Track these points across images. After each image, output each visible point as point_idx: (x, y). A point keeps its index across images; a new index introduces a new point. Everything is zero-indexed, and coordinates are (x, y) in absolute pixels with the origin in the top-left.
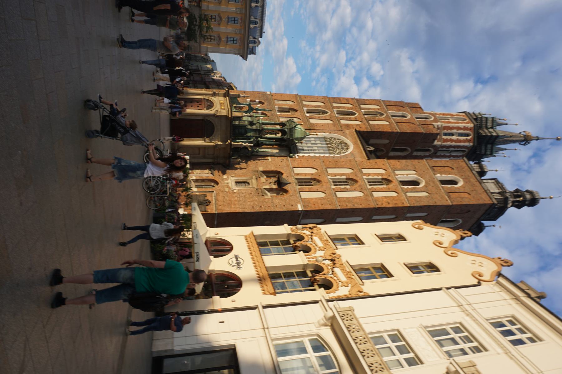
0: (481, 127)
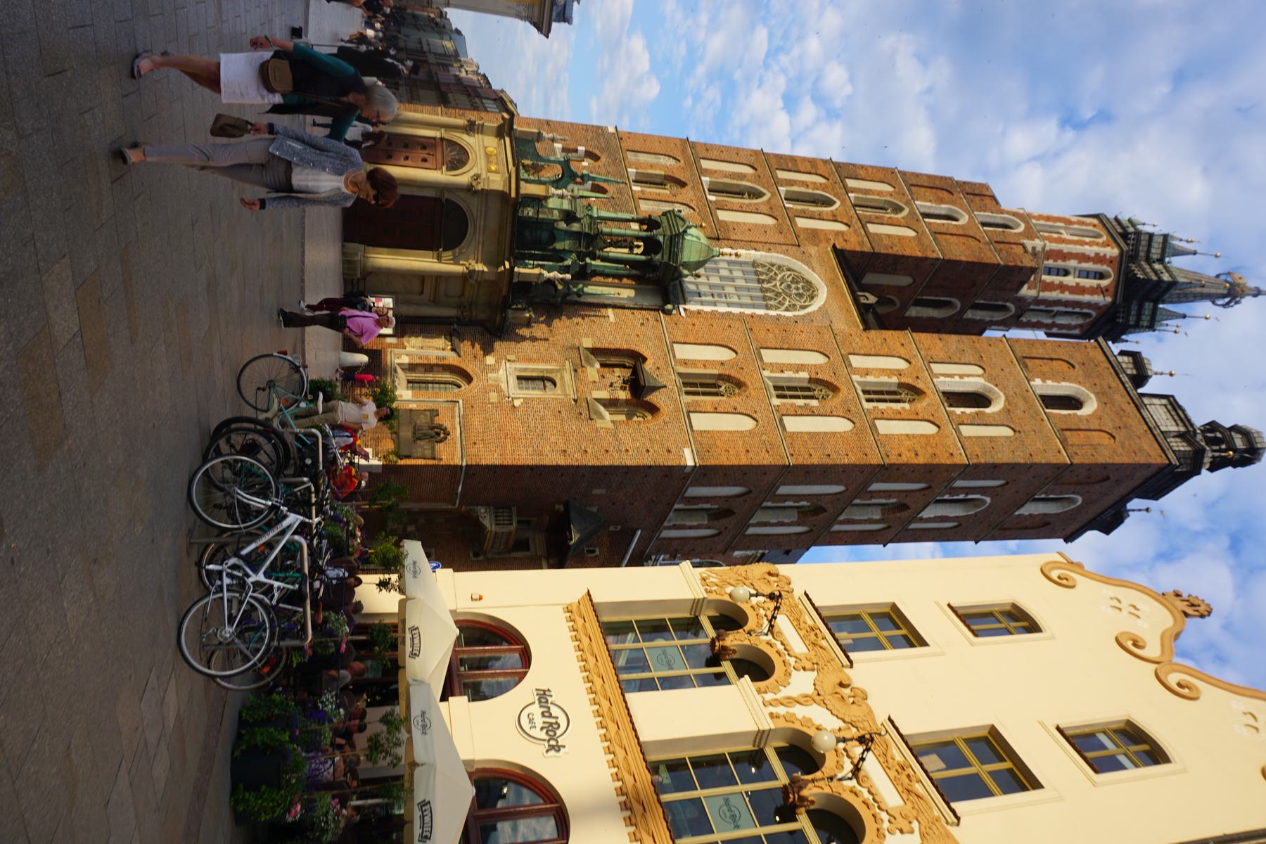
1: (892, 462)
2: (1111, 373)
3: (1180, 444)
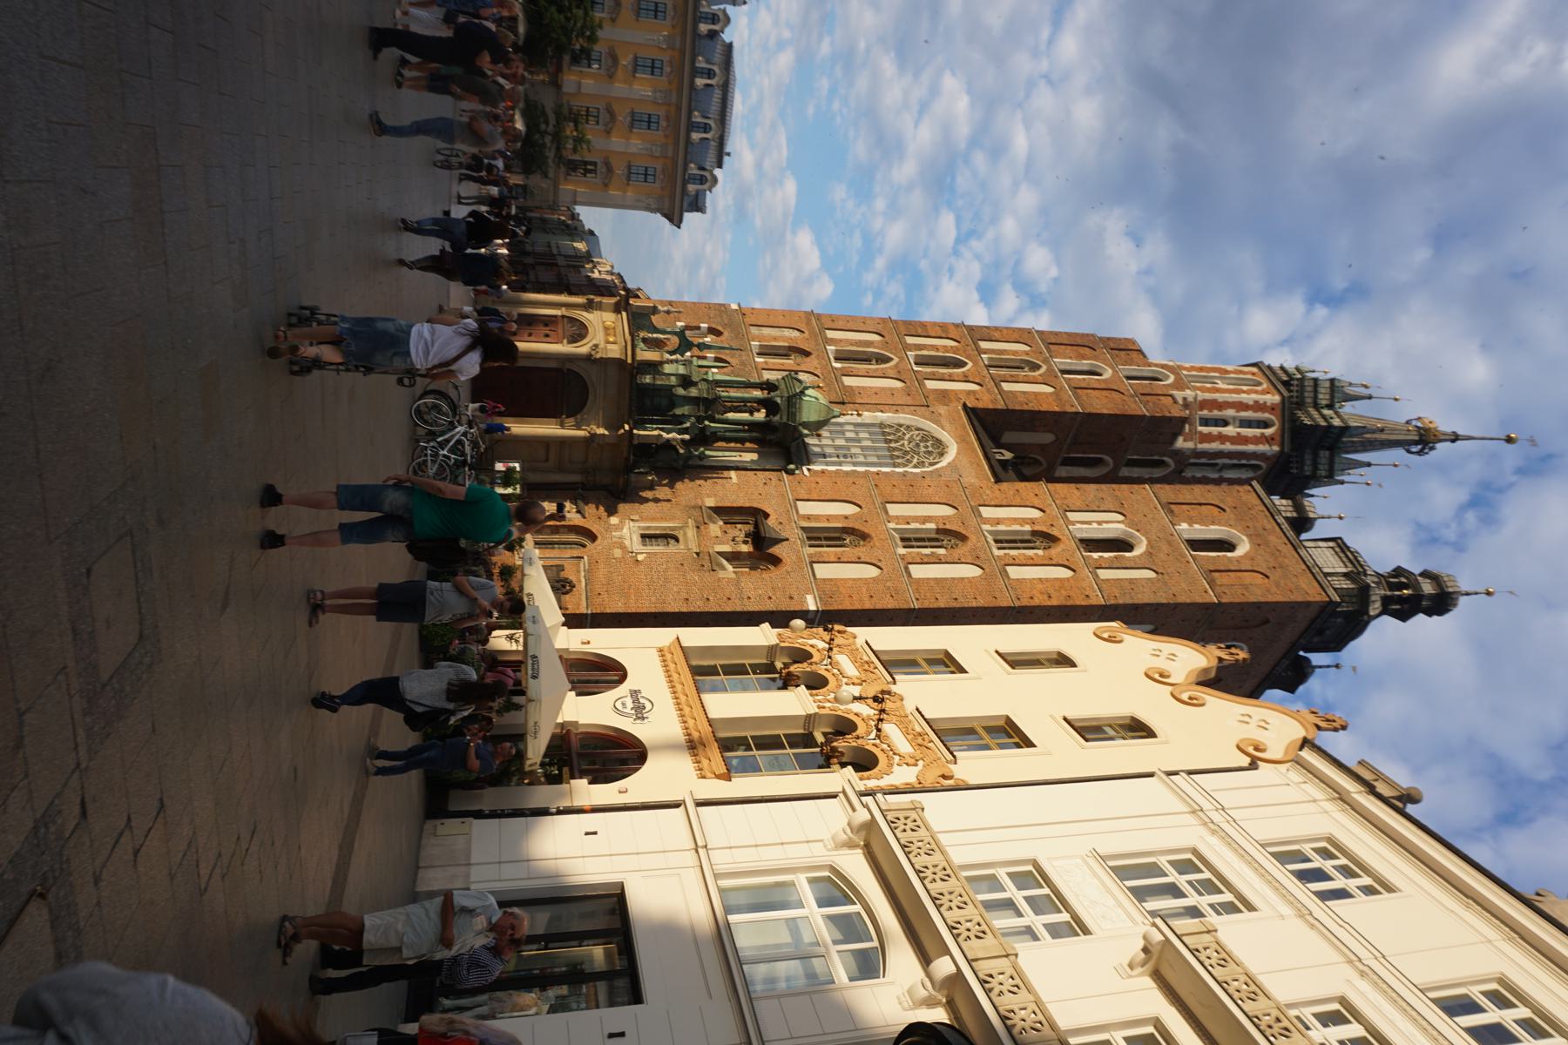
0: (1300, 404)
1: (1024, 604)
2: (1266, 516)
3: (1343, 582)
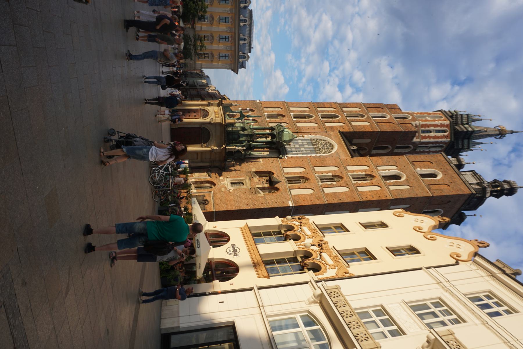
0: (457, 124)
1: (364, 200)
2: (447, 164)
3: (476, 186)
